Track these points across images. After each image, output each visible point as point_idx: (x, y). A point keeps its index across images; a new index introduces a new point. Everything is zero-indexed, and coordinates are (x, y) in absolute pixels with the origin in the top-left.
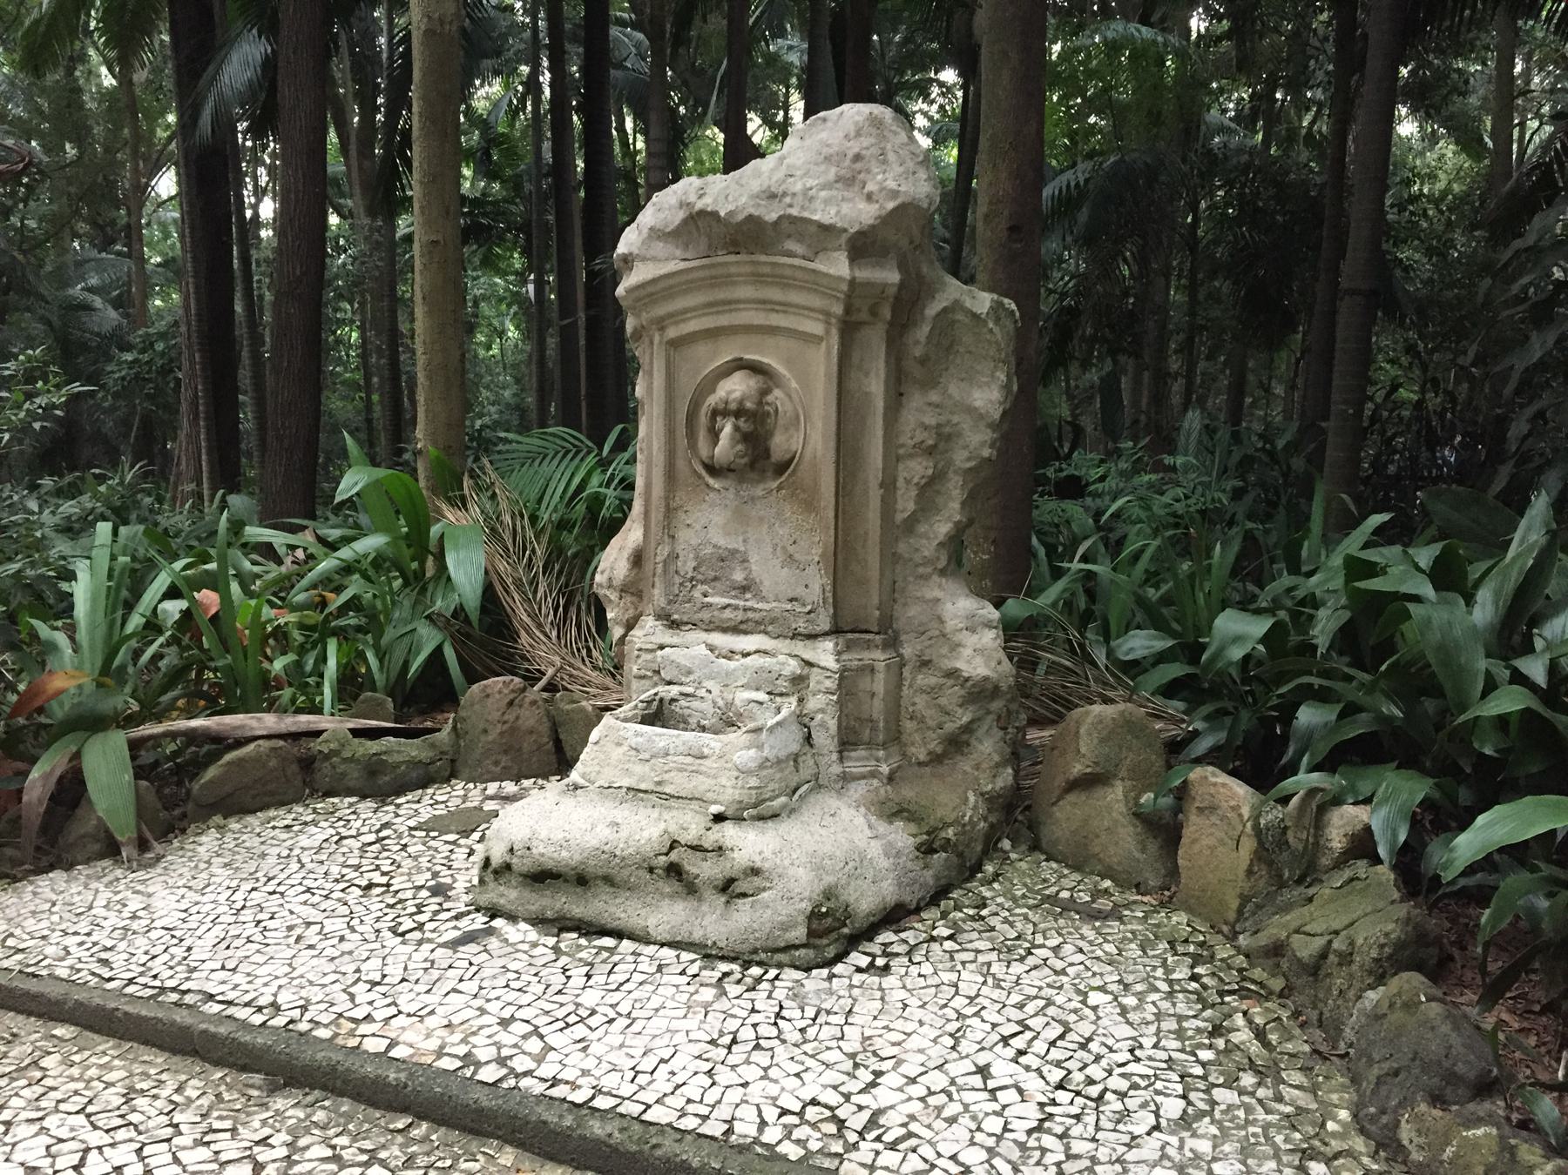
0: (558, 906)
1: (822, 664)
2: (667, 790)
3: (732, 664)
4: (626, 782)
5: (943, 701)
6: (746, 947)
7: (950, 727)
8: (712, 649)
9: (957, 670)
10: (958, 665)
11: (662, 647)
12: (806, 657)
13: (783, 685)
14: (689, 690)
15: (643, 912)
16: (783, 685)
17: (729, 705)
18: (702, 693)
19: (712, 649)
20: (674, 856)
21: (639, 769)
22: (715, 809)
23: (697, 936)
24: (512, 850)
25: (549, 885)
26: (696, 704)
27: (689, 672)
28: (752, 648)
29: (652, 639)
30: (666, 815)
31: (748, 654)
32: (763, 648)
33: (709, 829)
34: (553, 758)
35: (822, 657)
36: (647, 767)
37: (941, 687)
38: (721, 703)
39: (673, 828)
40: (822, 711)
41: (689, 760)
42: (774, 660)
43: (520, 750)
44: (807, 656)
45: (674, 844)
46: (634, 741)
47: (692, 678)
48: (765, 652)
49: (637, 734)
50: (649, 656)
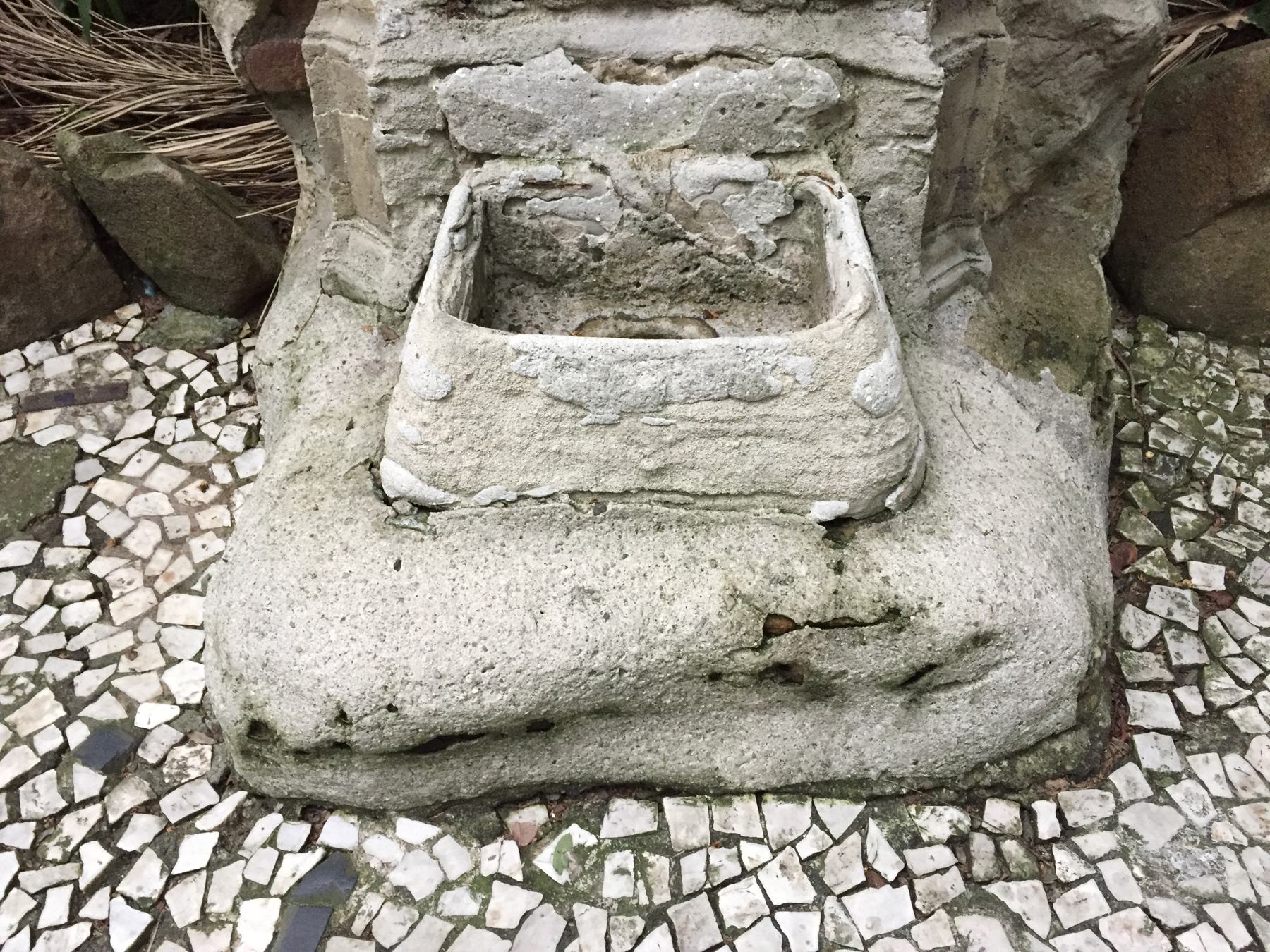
0: (485, 776)
1: (902, 70)
2: (685, 483)
3: (647, 94)
4: (563, 480)
5: (1052, 88)
6: (961, 766)
7: (1059, 139)
8: (580, 57)
9: (1102, 20)
10: (1107, 10)
11: (443, 69)
12: (851, 54)
13: (793, 131)
14: (548, 171)
15: (701, 744)
16: (793, 131)
17: (665, 195)
18: (580, 173)
19: (580, 57)
20: (782, 649)
21: (589, 445)
22: (825, 510)
23: (842, 767)
24: (342, 717)
25: (456, 754)
26: (571, 203)
27: (536, 126)
28: (702, 46)
29: (410, 48)
30: (709, 547)
31: (687, 64)
32: (729, 43)
33: (839, 568)
34: (109, 274)
35: (898, 52)
36: (612, 439)
37: (1052, 60)
38: (642, 195)
39: (750, 584)
40: (891, 179)
41: (729, 409)
42: (768, 73)
43: (33, 277)
44: (853, 54)
45: (774, 626)
46: (562, 383)
47: (543, 139)
48: (733, 54)
49: (562, 365)
50: (411, 97)
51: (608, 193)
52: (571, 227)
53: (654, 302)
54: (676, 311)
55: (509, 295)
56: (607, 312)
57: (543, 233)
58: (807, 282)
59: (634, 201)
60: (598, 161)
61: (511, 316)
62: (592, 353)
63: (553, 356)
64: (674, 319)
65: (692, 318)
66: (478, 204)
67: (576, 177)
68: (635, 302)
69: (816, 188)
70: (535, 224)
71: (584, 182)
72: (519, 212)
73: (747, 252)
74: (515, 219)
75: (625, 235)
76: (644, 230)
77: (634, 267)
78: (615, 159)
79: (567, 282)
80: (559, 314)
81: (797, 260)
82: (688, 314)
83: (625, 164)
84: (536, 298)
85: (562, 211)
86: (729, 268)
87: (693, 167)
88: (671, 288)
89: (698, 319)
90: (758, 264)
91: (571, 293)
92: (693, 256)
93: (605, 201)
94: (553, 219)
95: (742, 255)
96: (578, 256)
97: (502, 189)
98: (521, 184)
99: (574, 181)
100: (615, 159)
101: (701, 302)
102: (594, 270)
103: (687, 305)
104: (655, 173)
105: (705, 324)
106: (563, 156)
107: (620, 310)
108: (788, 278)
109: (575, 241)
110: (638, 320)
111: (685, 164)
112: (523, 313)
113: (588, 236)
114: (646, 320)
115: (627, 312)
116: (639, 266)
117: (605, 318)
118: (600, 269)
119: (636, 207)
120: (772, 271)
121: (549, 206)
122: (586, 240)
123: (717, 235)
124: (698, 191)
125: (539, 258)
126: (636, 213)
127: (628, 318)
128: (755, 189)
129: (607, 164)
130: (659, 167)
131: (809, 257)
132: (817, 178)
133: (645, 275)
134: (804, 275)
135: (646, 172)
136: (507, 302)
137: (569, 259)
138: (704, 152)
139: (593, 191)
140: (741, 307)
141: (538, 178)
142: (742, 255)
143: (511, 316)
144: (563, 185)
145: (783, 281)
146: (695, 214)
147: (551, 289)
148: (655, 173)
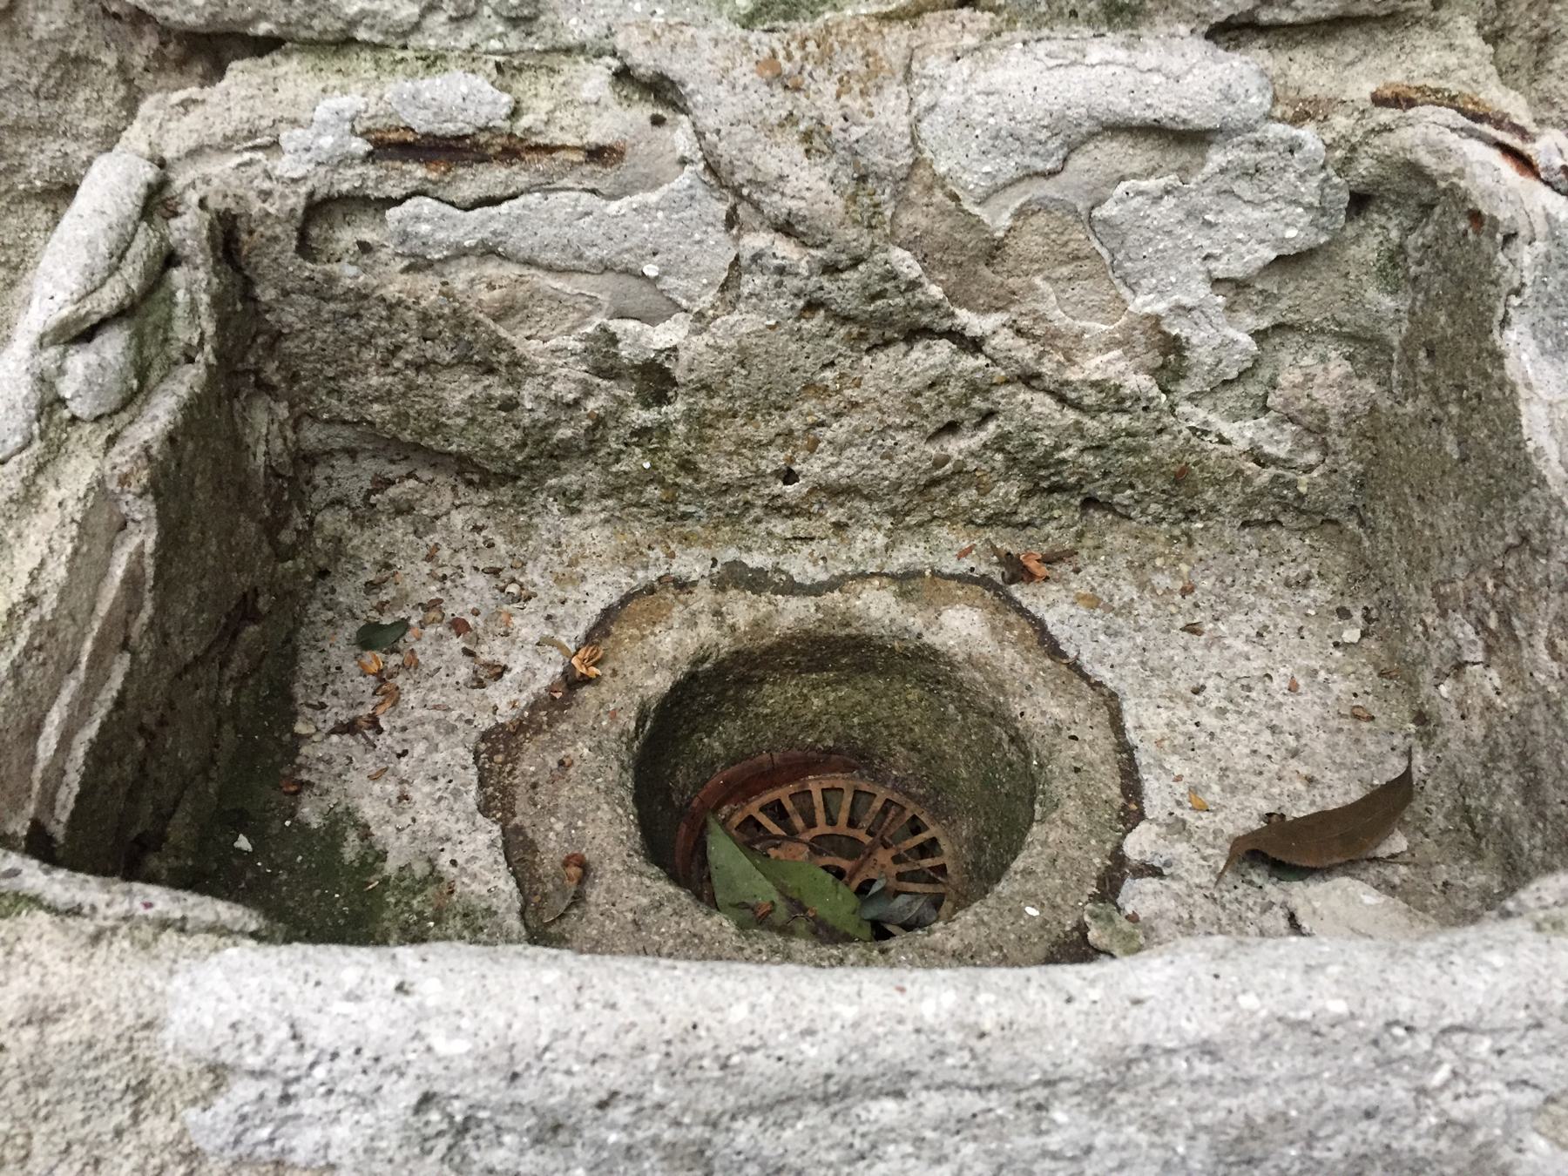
51: (685, 178)
52: (556, 298)
53: (839, 526)
54: (910, 554)
55: (365, 516)
56: (691, 564)
57: (460, 320)
58: (1351, 467)
59: (778, 204)
60: (644, 60)
61: (371, 587)
62: (613, 1076)
63: (403, 1095)
64: (906, 582)
65: (963, 579)
66: (188, 228)
67: (564, 118)
68: (781, 527)
69: (1442, 153)
70: (427, 288)
71: (594, 137)
72: (365, 247)
73: (1153, 373)
74: (349, 274)
75: (745, 322)
76: (812, 306)
77: (776, 424)
78: (707, 51)
79: (557, 472)
80: (533, 574)
81: (1331, 400)
82: (950, 565)
83: (745, 72)
84: (458, 518)
85: (519, 240)
86: (1089, 423)
87: (997, 76)
88: (896, 486)
89: (984, 581)
90: (1185, 408)
91: (572, 502)
92: (974, 388)
93: (670, 205)
94: (491, 269)
95: (1139, 382)
96: (588, 394)
97: (286, 166)
98: (360, 146)
99: (555, 136)
100: (707, 51)
101: (990, 521)
102: (642, 432)
103: (942, 532)
104: (855, 104)
105: (1010, 599)
106: (514, 41)
107: (731, 554)
108: (1281, 451)
109: (572, 343)
110: (793, 588)
111: (965, 65)
112: (415, 577)
113: (615, 325)
114: (816, 589)
115: (755, 560)
116: (793, 421)
117: (683, 586)
118: (664, 430)
119: (786, 228)
120: (1228, 430)
121: (471, 227)
122: (613, 340)
123: (1059, 318)
124: (1009, 168)
125: (455, 400)
126: (786, 250)
127: (756, 582)
128: (1217, 158)
129: (675, 68)
130: (872, 78)
131: (1369, 386)
132: (1449, 115)
133: (813, 447)
134: (1343, 445)
135: (823, 99)
136: (358, 538)
137: (555, 403)
138: (1037, 23)
139: (626, 172)
140: (1116, 539)
141: (422, 122)
142: (1139, 382)
143: (371, 587)
144: (514, 151)
145: (1262, 460)
146: (994, 251)
147: (505, 493)
148: (855, 104)
